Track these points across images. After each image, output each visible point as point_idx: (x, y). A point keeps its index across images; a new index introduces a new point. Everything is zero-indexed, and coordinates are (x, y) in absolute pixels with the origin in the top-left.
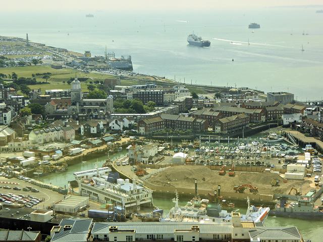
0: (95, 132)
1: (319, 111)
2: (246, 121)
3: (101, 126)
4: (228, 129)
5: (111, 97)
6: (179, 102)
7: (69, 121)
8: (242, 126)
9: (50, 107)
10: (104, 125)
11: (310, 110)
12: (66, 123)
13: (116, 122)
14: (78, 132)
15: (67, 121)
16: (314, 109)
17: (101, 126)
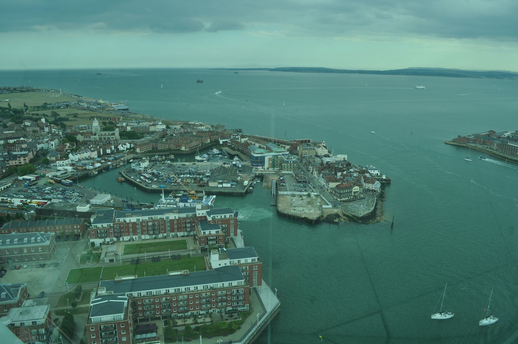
0: (110, 152)
1: (239, 135)
2: (199, 143)
3: (113, 149)
4: (189, 148)
5: (117, 129)
6: (159, 132)
7: (93, 146)
8: (197, 145)
9: (80, 138)
10: (115, 147)
11: (234, 135)
12: (91, 148)
13: (122, 146)
14: (99, 152)
15: (92, 146)
16: (236, 134)
17: (113, 149)
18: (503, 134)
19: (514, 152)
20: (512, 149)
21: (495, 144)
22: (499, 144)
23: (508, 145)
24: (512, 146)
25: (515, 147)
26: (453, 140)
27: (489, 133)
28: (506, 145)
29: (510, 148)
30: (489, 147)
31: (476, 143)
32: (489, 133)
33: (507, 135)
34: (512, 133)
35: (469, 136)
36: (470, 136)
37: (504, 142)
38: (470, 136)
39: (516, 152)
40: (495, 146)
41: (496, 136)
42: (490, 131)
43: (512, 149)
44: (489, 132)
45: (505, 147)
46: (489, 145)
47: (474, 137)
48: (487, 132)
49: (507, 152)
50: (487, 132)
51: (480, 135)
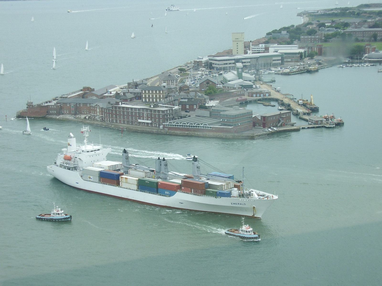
18: (107, 90)
19: (132, 118)
20: (128, 112)
21: (98, 110)
22: (104, 109)
23: (119, 108)
24: (127, 108)
25: (132, 108)
26: (19, 114)
27: (82, 92)
28: (116, 107)
29: (123, 112)
30: (87, 117)
31: (63, 114)
32: (82, 92)
33: (114, 93)
34: (123, 87)
35: (47, 102)
36: (50, 102)
37: (112, 104)
38: (50, 102)
39: (136, 119)
40: (98, 114)
41: (97, 96)
42: (85, 89)
43: (128, 112)
44: (81, 90)
45: (116, 111)
46: (87, 114)
47: (57, 103)
48: (79, 91)
49: (120, 121)
50: (79, 91)
51: (66, 97)
